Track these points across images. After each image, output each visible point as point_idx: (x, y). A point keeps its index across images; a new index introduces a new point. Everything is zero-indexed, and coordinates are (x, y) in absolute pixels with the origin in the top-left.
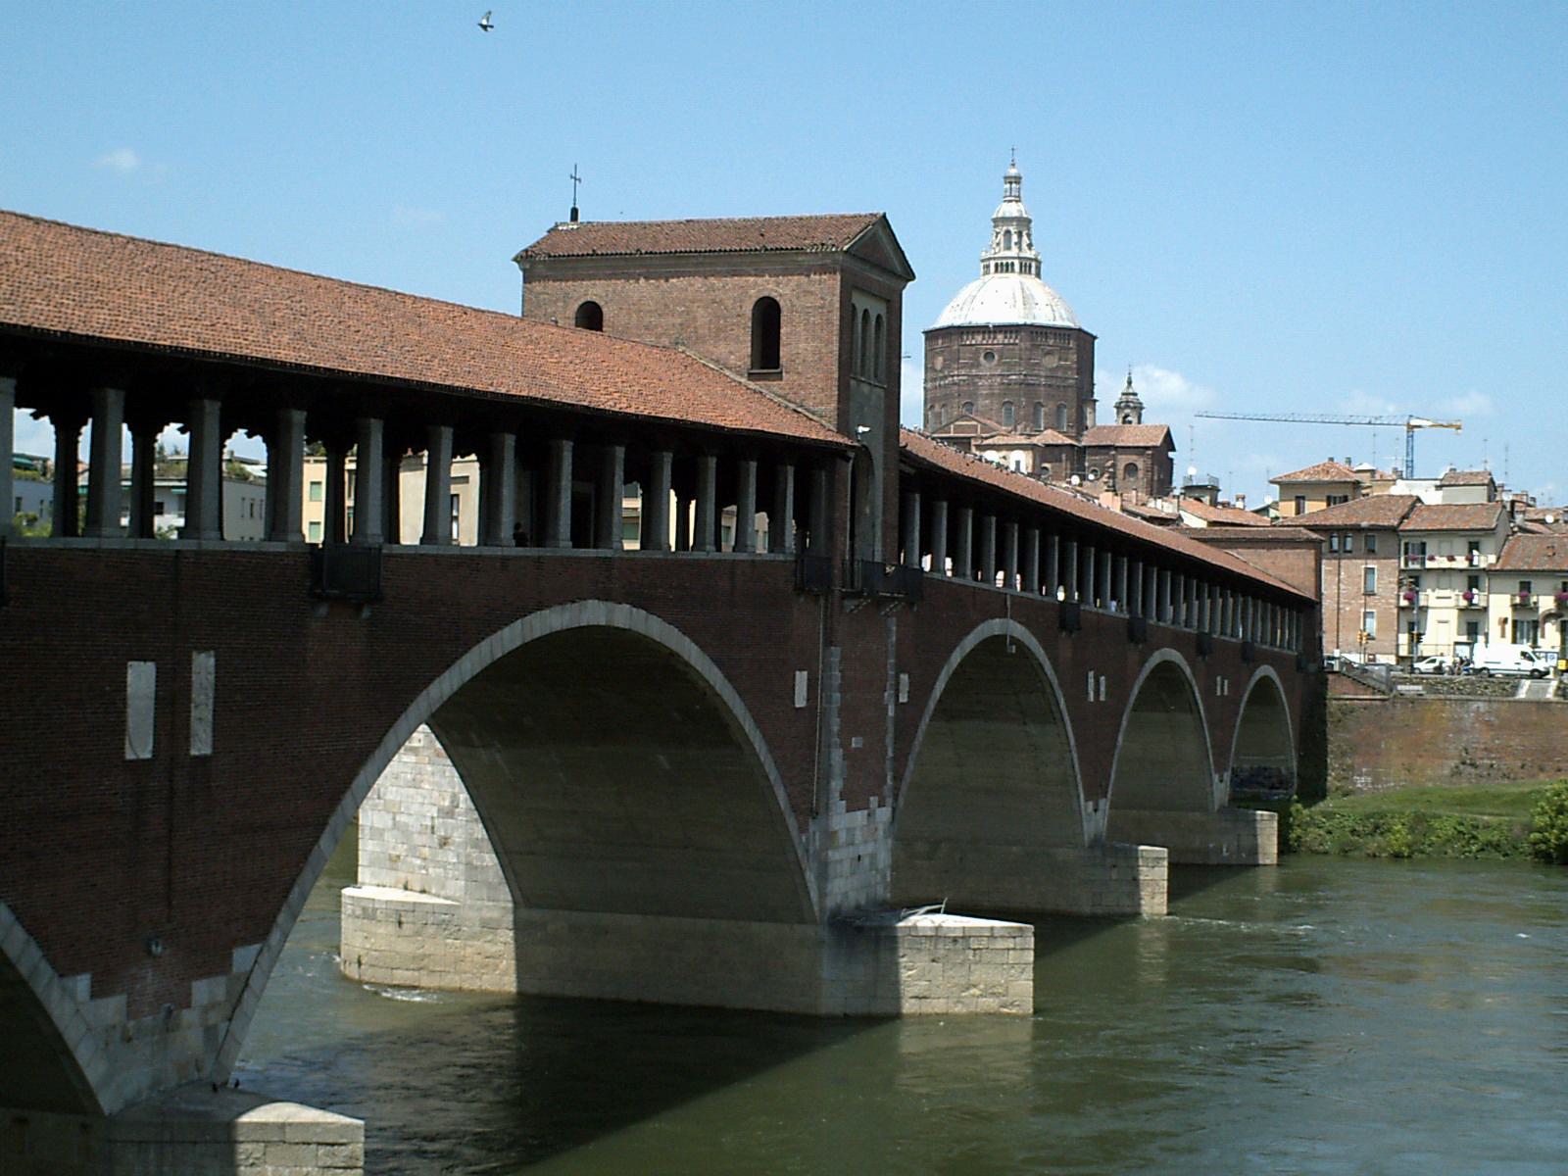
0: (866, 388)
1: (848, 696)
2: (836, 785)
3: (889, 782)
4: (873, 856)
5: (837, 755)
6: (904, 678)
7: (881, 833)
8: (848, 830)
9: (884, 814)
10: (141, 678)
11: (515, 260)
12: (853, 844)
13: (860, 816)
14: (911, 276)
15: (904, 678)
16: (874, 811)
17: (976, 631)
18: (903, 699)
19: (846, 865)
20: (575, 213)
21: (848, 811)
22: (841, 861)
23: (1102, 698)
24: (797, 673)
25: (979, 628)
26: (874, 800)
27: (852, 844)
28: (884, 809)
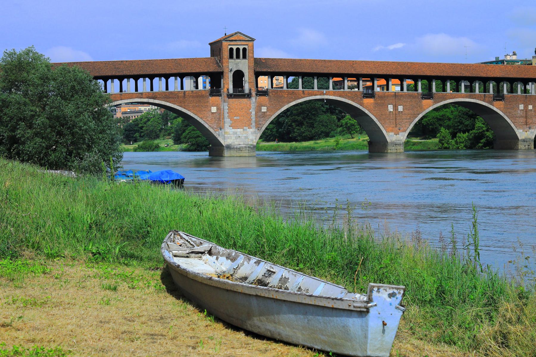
0: (238, 61)
1: (232, 110)
2: (227, 125)
3: (254, 124)
4: (246, 137)
7: (250, 133)
8: (233, 132)
11: (210, 44)
12: (236, 134)
13: (239, 130)
14: (253, 40)
16: (246, 129)
19: (233, 138)
20: (225, 34)
22: (231, 137)
24: (212, 107)
27: (236, 134)
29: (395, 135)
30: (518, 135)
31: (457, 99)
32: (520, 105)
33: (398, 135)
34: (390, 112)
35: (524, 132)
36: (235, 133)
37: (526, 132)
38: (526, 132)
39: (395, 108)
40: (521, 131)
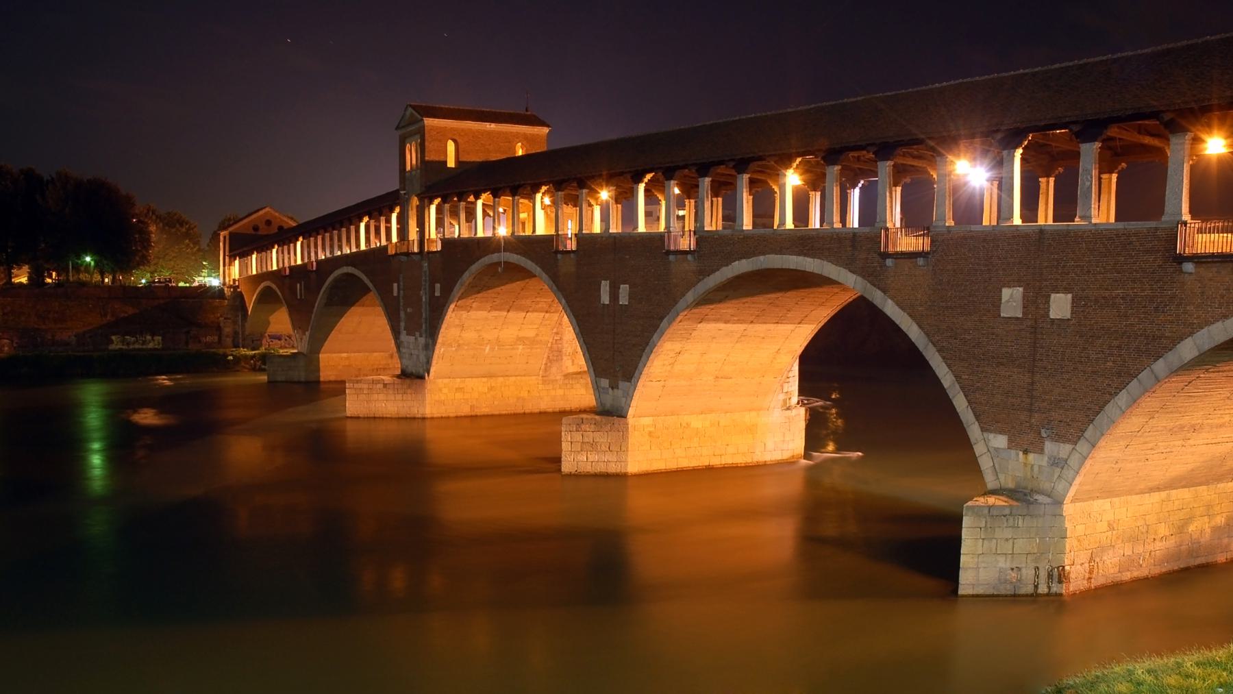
2: (402, 324)
4: (418, 356)
5: (402, 315)
6: (438, 286)
7: (420, 348)
9: (422, 340)
10: (298, 285)
13: (412, 339)
15: (438, 286)
17: (480, 261)
18: (437, 294)
21: (407, 335)
22: (405, 353)
23: (624, 300)
25: (483, 259)
26: (417, 334)
28: (421, 338)
29: (610, 389)
30: (985, 463)
31: (762, 258)
32: (1006, 293)
33: (615, 390)
34: (604, 305)
35: (1013, 452)
36: (408, 348)
37: (1026, 452)
38: (1026, 452)
39: (614, 295)
40: (1000, 441)
